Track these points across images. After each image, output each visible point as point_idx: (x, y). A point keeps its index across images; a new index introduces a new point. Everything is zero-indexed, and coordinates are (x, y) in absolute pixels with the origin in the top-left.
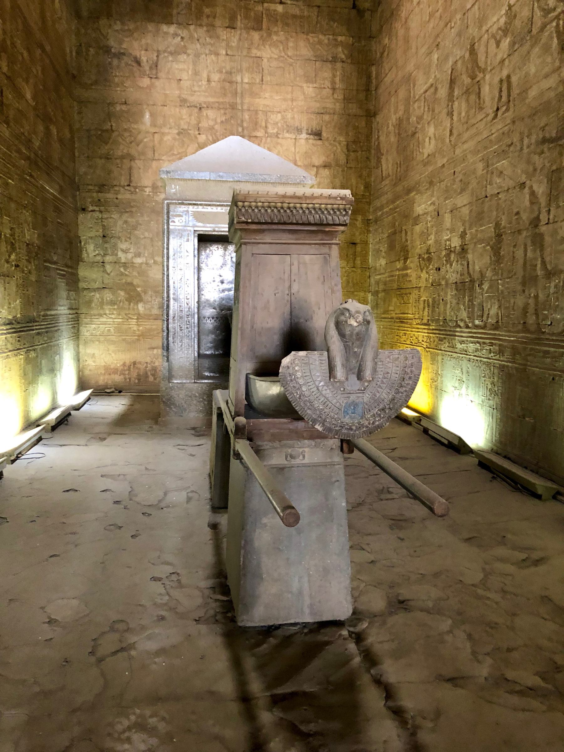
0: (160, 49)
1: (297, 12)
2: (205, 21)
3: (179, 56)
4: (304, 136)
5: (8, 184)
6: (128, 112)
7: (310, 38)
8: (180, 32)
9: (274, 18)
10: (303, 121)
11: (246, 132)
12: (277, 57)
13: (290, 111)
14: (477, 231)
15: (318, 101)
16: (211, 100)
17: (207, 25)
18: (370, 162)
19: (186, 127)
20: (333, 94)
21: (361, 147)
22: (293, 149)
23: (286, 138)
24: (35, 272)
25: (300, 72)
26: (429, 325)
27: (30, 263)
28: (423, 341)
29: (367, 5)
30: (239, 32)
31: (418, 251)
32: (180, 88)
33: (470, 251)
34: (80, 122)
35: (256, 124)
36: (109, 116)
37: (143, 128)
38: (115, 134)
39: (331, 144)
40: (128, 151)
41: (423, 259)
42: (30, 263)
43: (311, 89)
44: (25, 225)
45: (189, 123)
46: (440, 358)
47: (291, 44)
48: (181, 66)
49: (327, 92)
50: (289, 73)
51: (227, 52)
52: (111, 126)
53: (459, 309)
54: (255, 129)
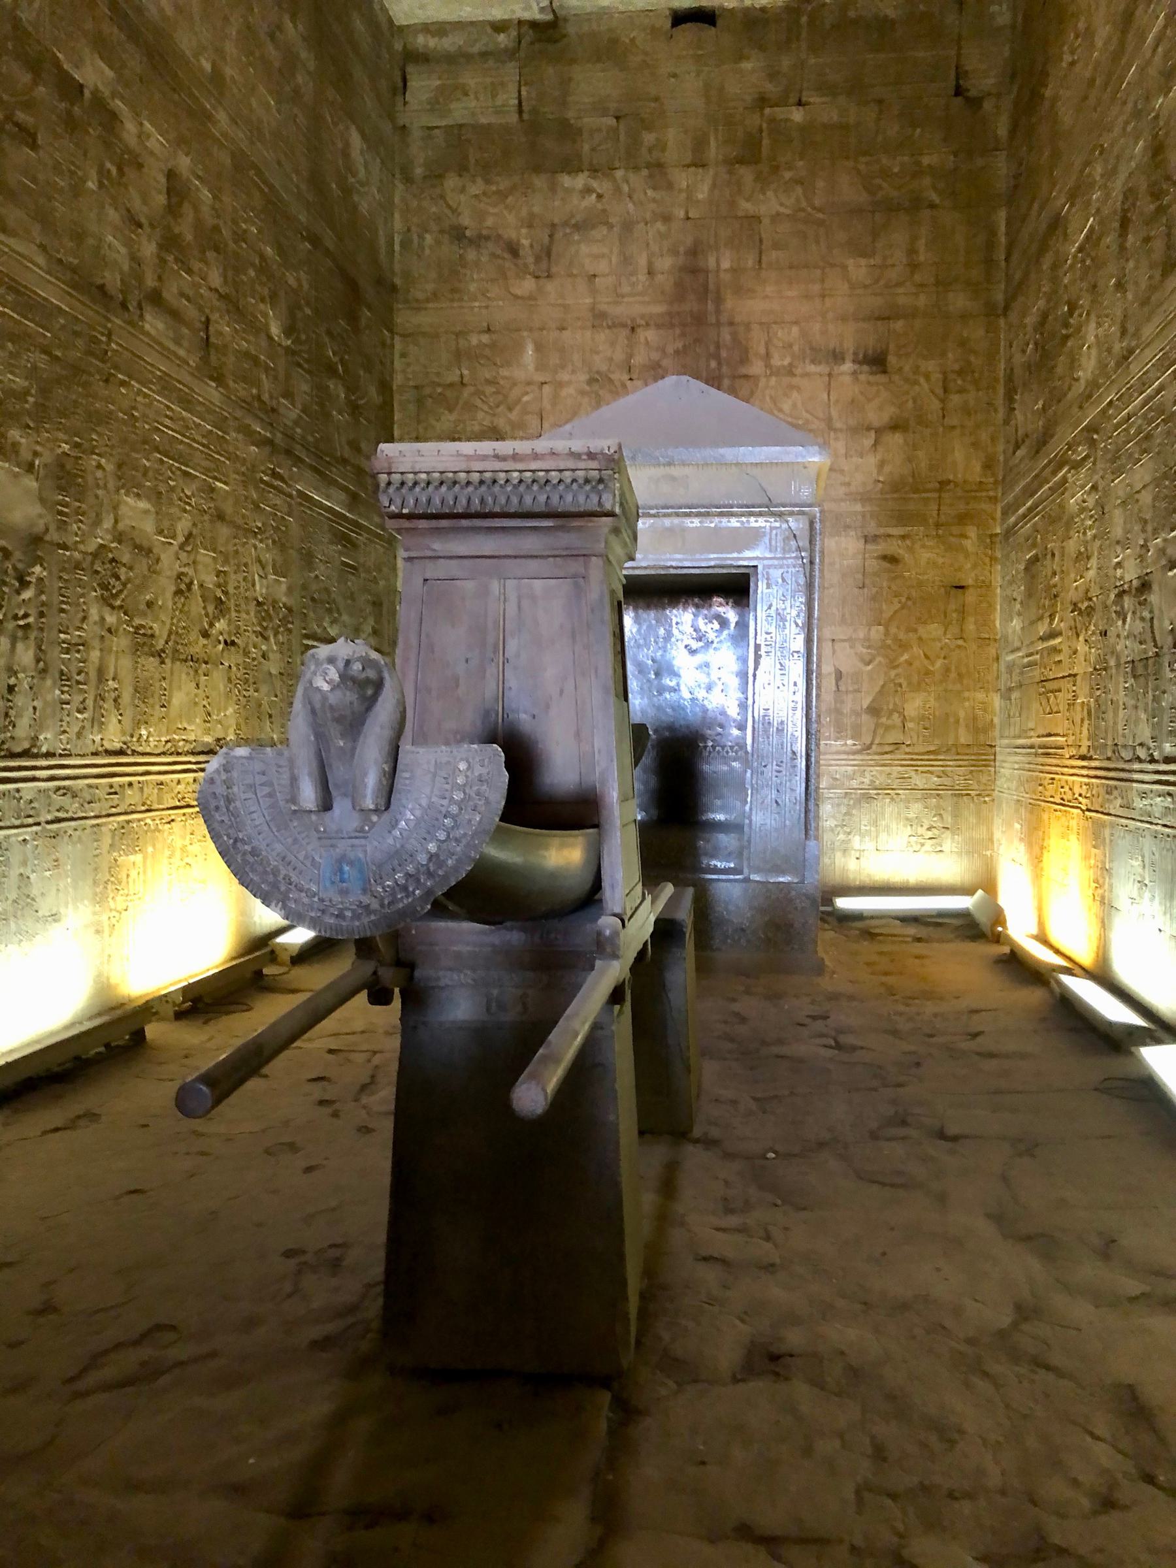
0: (556, 221)
3: (593, 232)
4: (848, 366)
5: (213, 490)
6: (493, 346)
7: (862, 167)
8: (595, 184)
10: (848, 337)
11: (724, 369)
12: (788, 212)
13: (820, 319)
14: (1165, 540)
15: (881, 294)
17: (648, 166)
18: (996, 411)
19: (604, 368)
20: (912, 273)
21: (976, 382)
22: (825, 396)
23: (806, 375)
24: (278, 656)
26: (1091, 758)
27: (266, 639)
28: (1080, 795)
30: (711, 172)
31: (1072, 595)
32: (594, 292)
33: (1155, 587)
34: (404, 371)
35: (746, 351)
36: (459, 356)
37: (519, 374)
38: (470, 389)
39: (907, 380)
40: (492, 422)
41: (1080, 613)
42: (266, 639)
43: (863, 270)
44: (255, 568)
45: (611, 359)
46: (1107, 832)
48: (595, 249)
50: (817, 242)
51: (687, 213)
52: (462, 376)
53: (1137, 721)
54: (744, 360)
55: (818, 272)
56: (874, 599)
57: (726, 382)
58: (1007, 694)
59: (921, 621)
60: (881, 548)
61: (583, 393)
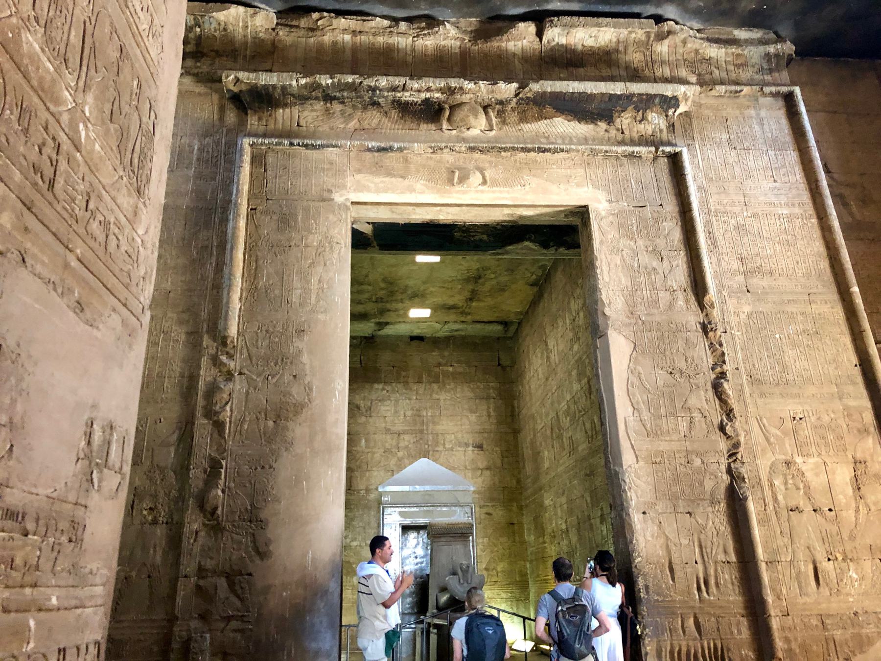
1: (461, 370)
2: (402, 379)
4: (471, 448)
9: (446, 374)
10: (469, 438)
16: (406, 428)
25: (466, 406)
29: (508, 363)
32: (386, 422)
35: (437, 442)
47: (459, 390)
48: (388, 408)
49: (484, 418)
54: (437, 445)
55: (459, 418)
56: (484, 528)
57: (431, 453)
58: (531, 562)
59: (501, 536)
60: (485, 510)
61: (381, 456)
